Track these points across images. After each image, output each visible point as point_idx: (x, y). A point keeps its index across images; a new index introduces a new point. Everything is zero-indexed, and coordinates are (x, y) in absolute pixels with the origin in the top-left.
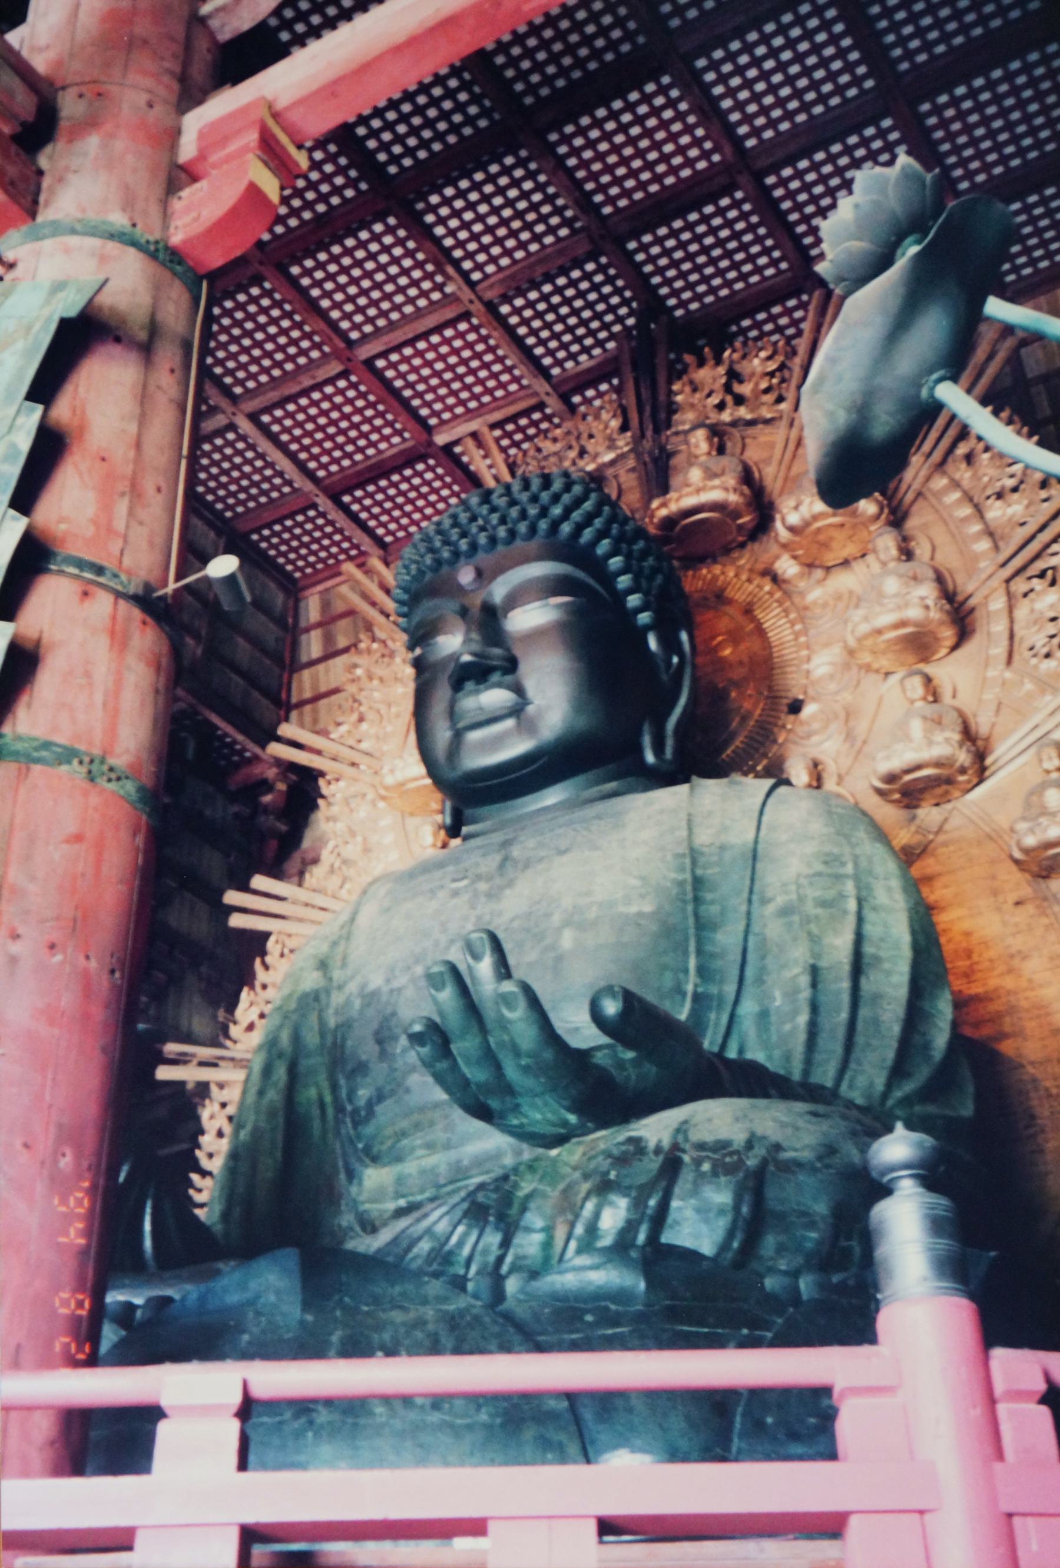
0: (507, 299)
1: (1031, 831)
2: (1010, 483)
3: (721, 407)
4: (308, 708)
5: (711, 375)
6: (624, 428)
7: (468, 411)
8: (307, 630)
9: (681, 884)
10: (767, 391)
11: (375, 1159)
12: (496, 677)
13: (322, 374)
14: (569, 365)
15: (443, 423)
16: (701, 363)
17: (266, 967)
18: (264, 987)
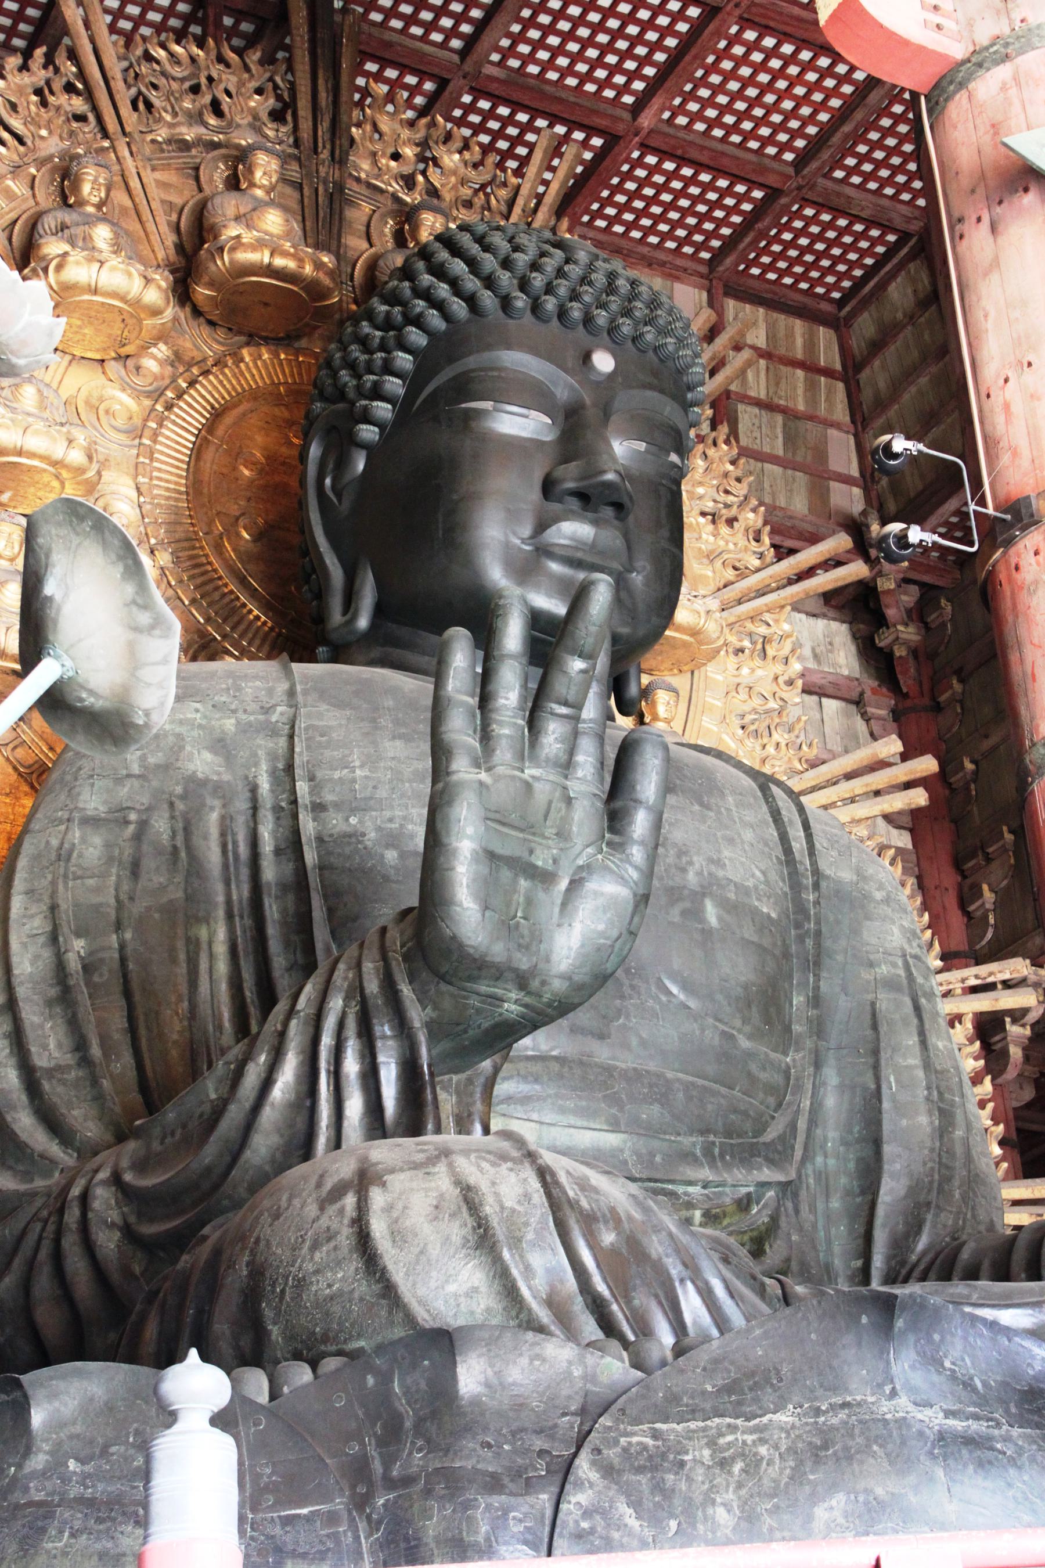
2: (726, 513)
6: (277, 116)
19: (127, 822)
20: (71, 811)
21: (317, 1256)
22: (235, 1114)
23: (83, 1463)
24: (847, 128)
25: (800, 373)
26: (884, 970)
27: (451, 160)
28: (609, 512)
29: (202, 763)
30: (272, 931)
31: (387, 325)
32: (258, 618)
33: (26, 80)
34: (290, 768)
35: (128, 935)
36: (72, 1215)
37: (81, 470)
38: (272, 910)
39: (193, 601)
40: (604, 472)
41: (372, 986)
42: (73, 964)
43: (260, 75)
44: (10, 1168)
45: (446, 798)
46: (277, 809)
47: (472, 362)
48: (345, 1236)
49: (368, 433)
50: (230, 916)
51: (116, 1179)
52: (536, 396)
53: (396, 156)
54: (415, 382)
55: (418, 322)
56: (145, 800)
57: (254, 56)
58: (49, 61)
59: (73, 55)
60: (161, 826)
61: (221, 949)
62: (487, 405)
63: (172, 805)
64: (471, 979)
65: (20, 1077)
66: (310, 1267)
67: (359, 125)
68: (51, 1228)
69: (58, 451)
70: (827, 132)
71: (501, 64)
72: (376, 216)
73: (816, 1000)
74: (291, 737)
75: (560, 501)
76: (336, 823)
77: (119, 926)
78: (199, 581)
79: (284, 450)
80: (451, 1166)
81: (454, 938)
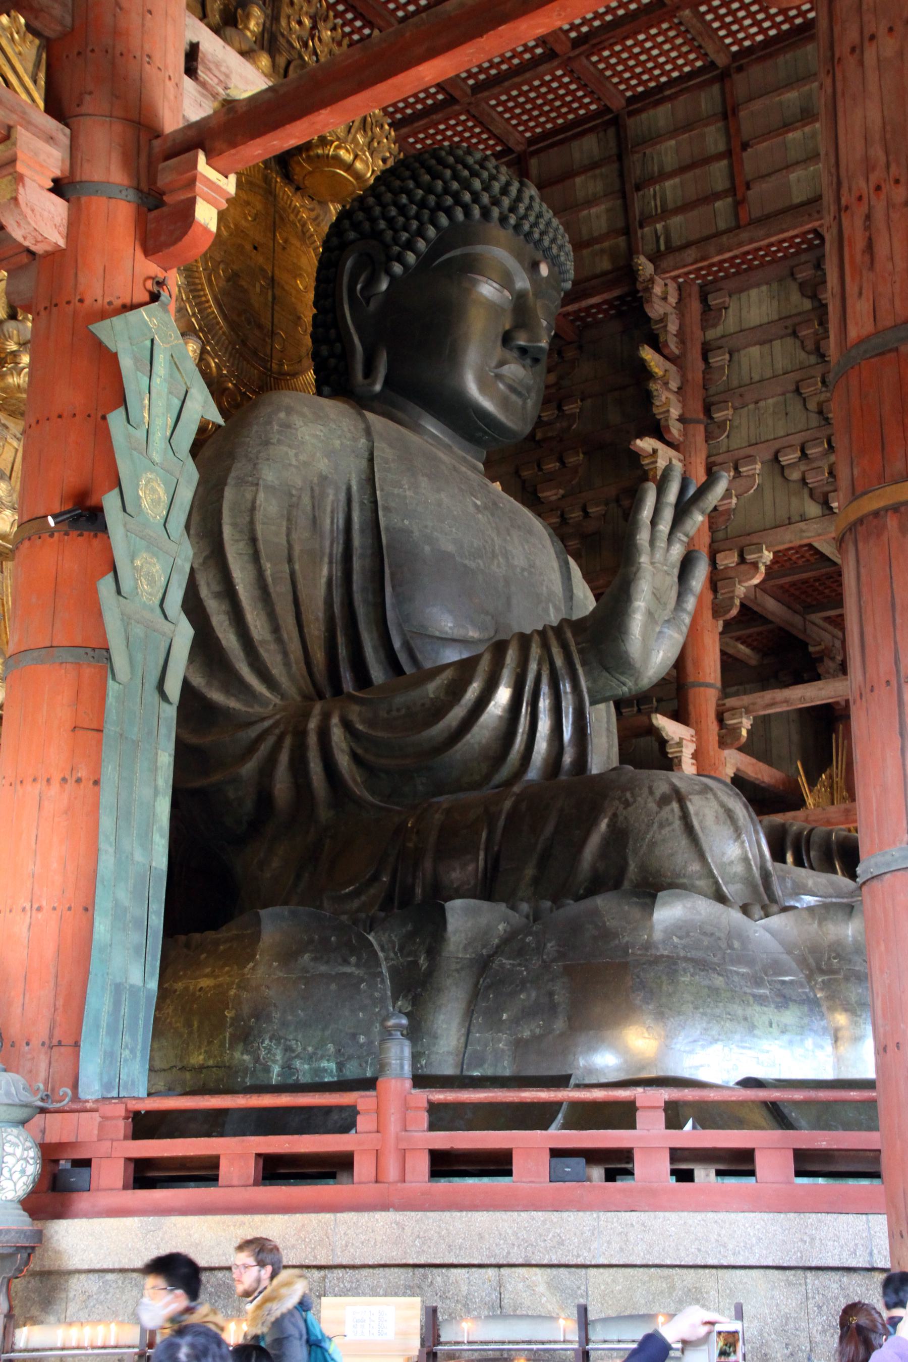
19: (291, 495)
20: (259, 479)
21: (663, 832)
22: (458, 713)
23: (680, 938)
28: (528, 361)
29: (323, 465)
30: (356, 577)
31: (422, 204)
32: (224, 333)
34: (370, 480)
35: (297, 567)
36: (312, 740)
38: (357, 564)
39: (194, 314)
40: (540, 341)
41: (559, 662)
42: (269, 580)
44: (233, 695)
45: (638, 575)
46: (362, 504)
47: (479, 249)
48: (677, 824)
49: (398, 268)
50: (330, 563)
51: (347, 725)
52: (506, 281)
54: (437, 249)
55: (449, 212)
56: (299, 483)
60: (306, 500)
61: (324, 580)
63: (312, 489)
64: (622, 674)
65: (238, 640)
66: (658, 837)
68: (288, 742)
72: (291, 68)
74: (371, 460)
75: (511, 350)
77: (290, 560)
78: (198, 300)
79: (243, 223)
80: (715, 795)
81: (626, 652)
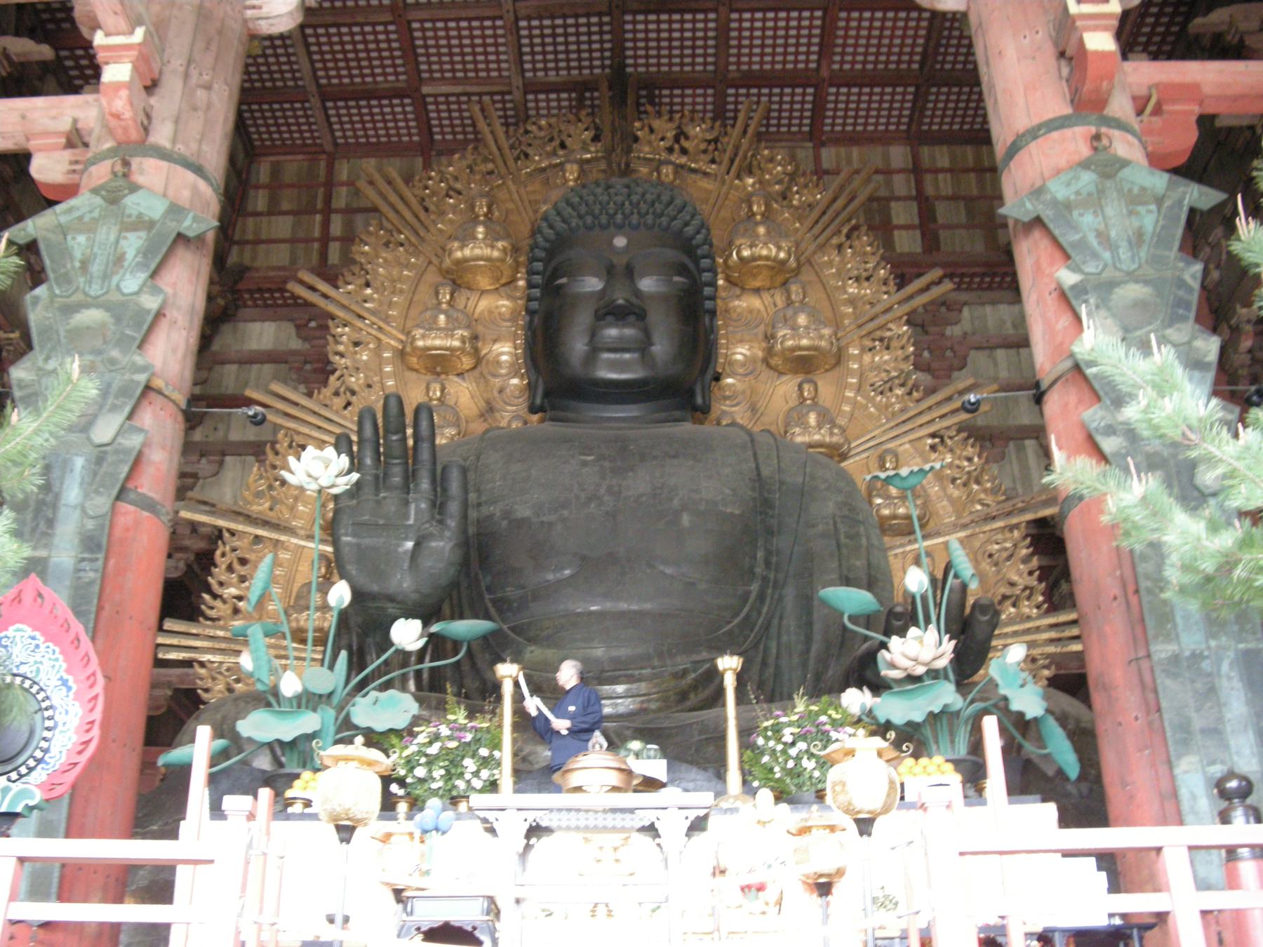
0: (529, 18)
1: (887, 506)
2: (865, 274)
3: (670, 150)
4: (248, 247)
5: (665, 127)
6: (596, 139)
7: (454, 78)
8: (257, 187)
9: (754, 499)
10: (705, 152)
11: (532, 641)
12: (632, 318)
13: (373, 18)
14: (541, 74)
15: (432, 79)
16: (659, 114)
17: (277, 453)
18: (274, 467)
24: (932, 44)
25: (972, 175)
26: (820, 527)
27: (696, 130)
33: (465, 163)
37: (463, 350)
43: (590, 119)
53: (663, 139)
57: (583, 113)
58: (475, 148)
59: (486, 146)
62: (564, 280)
67: (642, 129)
69: (449, 343)
70: (925, 46)
71: (738, 70)
73: (769, 553)
76: (485, 511)
